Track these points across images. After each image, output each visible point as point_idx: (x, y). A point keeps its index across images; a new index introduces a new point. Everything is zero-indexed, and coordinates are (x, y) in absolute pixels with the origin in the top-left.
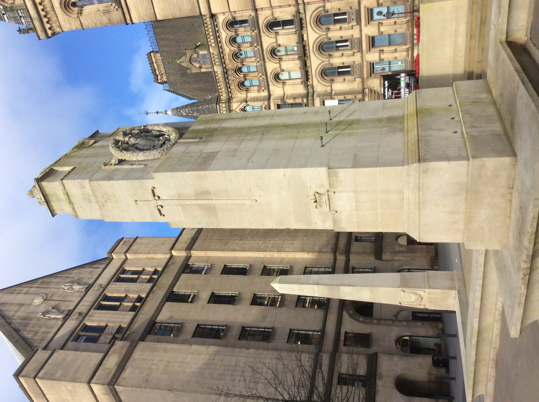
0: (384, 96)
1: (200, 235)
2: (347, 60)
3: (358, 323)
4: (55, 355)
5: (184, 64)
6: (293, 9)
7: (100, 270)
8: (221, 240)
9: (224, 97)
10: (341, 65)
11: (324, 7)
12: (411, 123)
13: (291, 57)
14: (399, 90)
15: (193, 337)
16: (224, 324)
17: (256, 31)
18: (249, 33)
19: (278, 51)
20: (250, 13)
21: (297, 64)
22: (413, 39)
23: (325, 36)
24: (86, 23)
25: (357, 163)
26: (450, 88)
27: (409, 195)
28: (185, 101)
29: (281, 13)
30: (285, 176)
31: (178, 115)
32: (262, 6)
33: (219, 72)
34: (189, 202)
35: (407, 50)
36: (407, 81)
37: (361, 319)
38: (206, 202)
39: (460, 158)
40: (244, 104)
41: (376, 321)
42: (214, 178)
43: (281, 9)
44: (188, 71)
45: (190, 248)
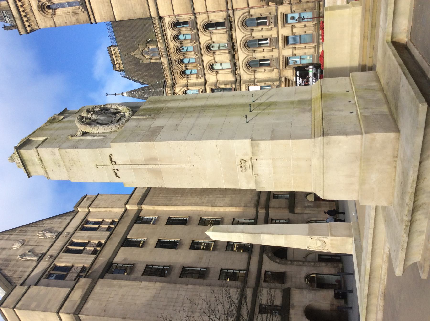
0: (296, 83)
2: (267, 55)
3: (276, 264)
4: (30, 289)
5: (137, 56)
6: (224, 14)
7: (68, 221)
8: (166, 196)
9: (169, 82)
10: (263, 58)
11: (249, 12)
12: (317, 105)
13: (223, 51)
14: (308, 79)
15: (143, 275)
16: (168, 264)
18: (189, 32)
19: (213, 47)
20: (190, 17)
21: (227, 57)
23: (250, 36)
24: (59, 22)
25: (274, 136)
26: (347, 78)
27: (316, 162)
28: (137, 86)
29: (215, 16)
30: (217, 146)
31: (132, 97)
32: (200, 11)
33: (165, 63)
34: (140, 167)
35: (314, 47)
36: (314, 72)
38: (154, 166)
39: (355, 133)
40: (185, 88)
41: (289, 262)
42: (160, 148)
43: (215, 14)
44: (141, 62)
45: (141, 203)
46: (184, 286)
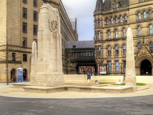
1: (56, 5)
9: (104, 12)
10: (111, 52)
16: (27, 17)
17: (123, 24)
22: (117, 74)
35: (114, 72)
40: (101, 19)
46: (20, 25)
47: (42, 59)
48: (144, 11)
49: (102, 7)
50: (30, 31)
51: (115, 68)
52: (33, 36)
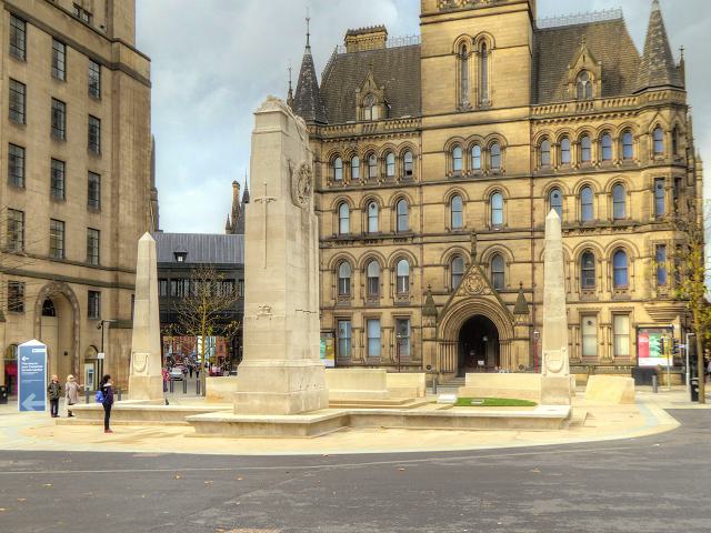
1: (140, 84)
5: (367, 84)
6: (417, 230)
11: (417, 266)
28: (320, 68)
29: (416, 216)
35: (361, 359)
37: (40, 303)
41: (38, 320)
47: (269, 310)
48: (475, 143)
49: (318, 111)
50: (35, 182)
51: (365, 342)
52: (48, 203)
